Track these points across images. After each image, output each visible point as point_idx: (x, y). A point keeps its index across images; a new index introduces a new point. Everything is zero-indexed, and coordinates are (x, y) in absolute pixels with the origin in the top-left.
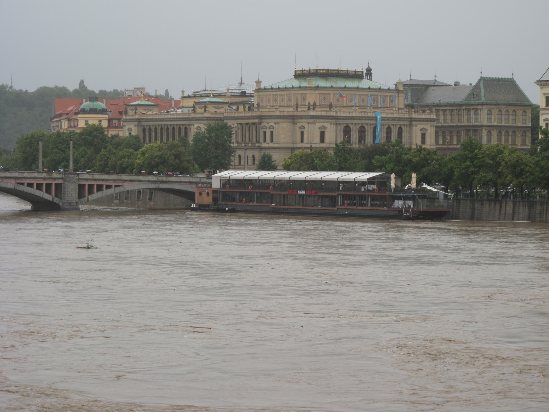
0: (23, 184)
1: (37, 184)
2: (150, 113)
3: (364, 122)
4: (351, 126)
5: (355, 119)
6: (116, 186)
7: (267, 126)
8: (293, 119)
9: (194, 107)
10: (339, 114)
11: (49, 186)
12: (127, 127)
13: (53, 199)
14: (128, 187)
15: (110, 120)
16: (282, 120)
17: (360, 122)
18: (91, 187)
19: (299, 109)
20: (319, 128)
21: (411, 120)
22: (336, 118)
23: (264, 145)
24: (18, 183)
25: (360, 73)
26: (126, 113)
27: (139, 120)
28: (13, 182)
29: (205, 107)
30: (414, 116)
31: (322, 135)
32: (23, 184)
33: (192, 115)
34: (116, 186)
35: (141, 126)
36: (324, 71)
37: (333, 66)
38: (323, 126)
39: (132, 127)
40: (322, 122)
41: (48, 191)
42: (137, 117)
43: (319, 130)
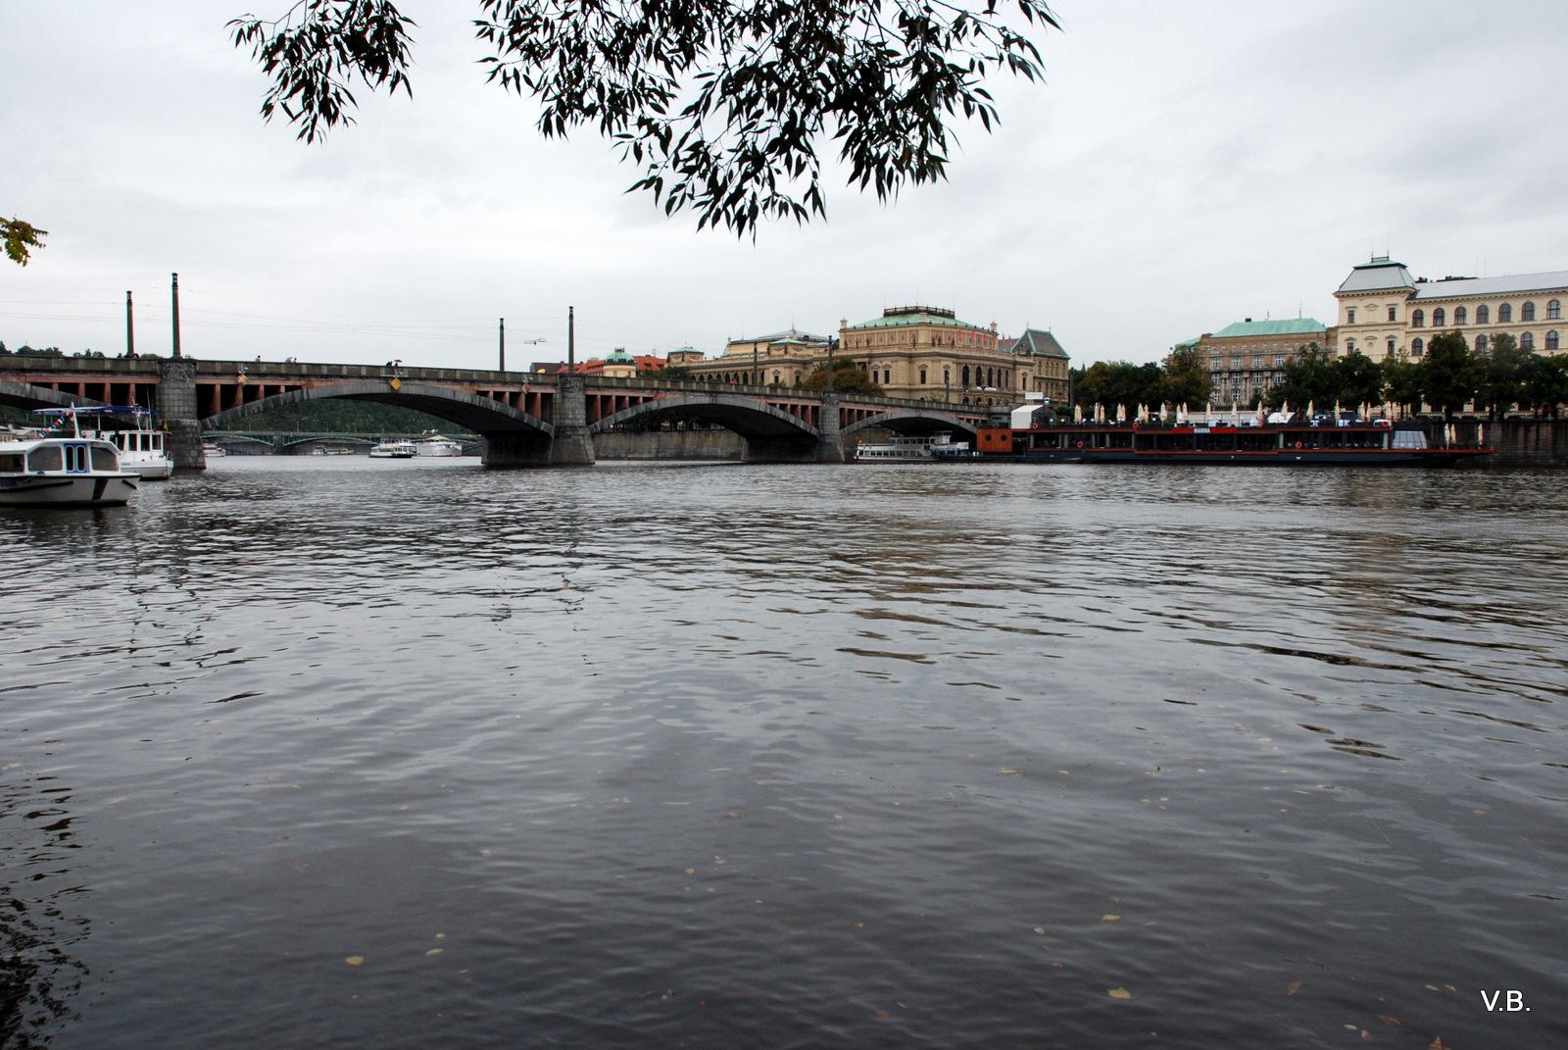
3: (981, 362)
7: (881, 365)
8: (910, 357)
16: (901, 358)
17: (978, 362)
21: (1015, 363)
29: (786, 349)
30: (1018, 359)
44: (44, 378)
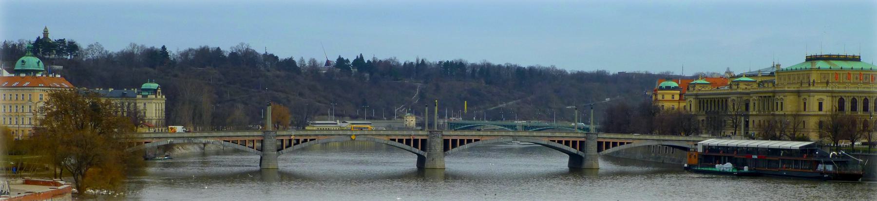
0: (554, 141)
1: (565, 141)
2: (703, 89)
3: (855, 94)
4: (845, 98)
5: (847, 93)
6: (627, 143)
9: (731, 85)
10: (834, 89)
11: (574, 143)
12: (689, 100)
13: (577, 152)
14: (636, 144)
15: (680, 95)
17: (852, 94)
18: (607, 144)
19: (803, 86)
20: (818, 100)
22: (832, 92)
23: (777, 113)
24: (551, 141)
25: (857, 57)
26: (688, 89)
27: (696, 95)
31: (820, 105)
32: (554, 141)
33: (730, 91)
34: (627, 143)
35: (698, 99)
36: (835, 57)
37: (834, 52)
38: (821, 98)
39: (692, 99)
40: (820, 95)
41: (574, 146)
42: (695, 92)
43: (817, 101)
44: (227, 139)
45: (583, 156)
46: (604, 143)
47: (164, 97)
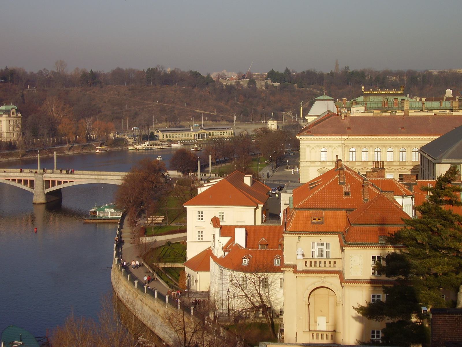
6: (70, 182)
11: (26, 182)
18: (54, 182)
24: (6, 179)
28: (4, 178)
45: (33, 192)
46: (50, 182)
47: (20, 115)
